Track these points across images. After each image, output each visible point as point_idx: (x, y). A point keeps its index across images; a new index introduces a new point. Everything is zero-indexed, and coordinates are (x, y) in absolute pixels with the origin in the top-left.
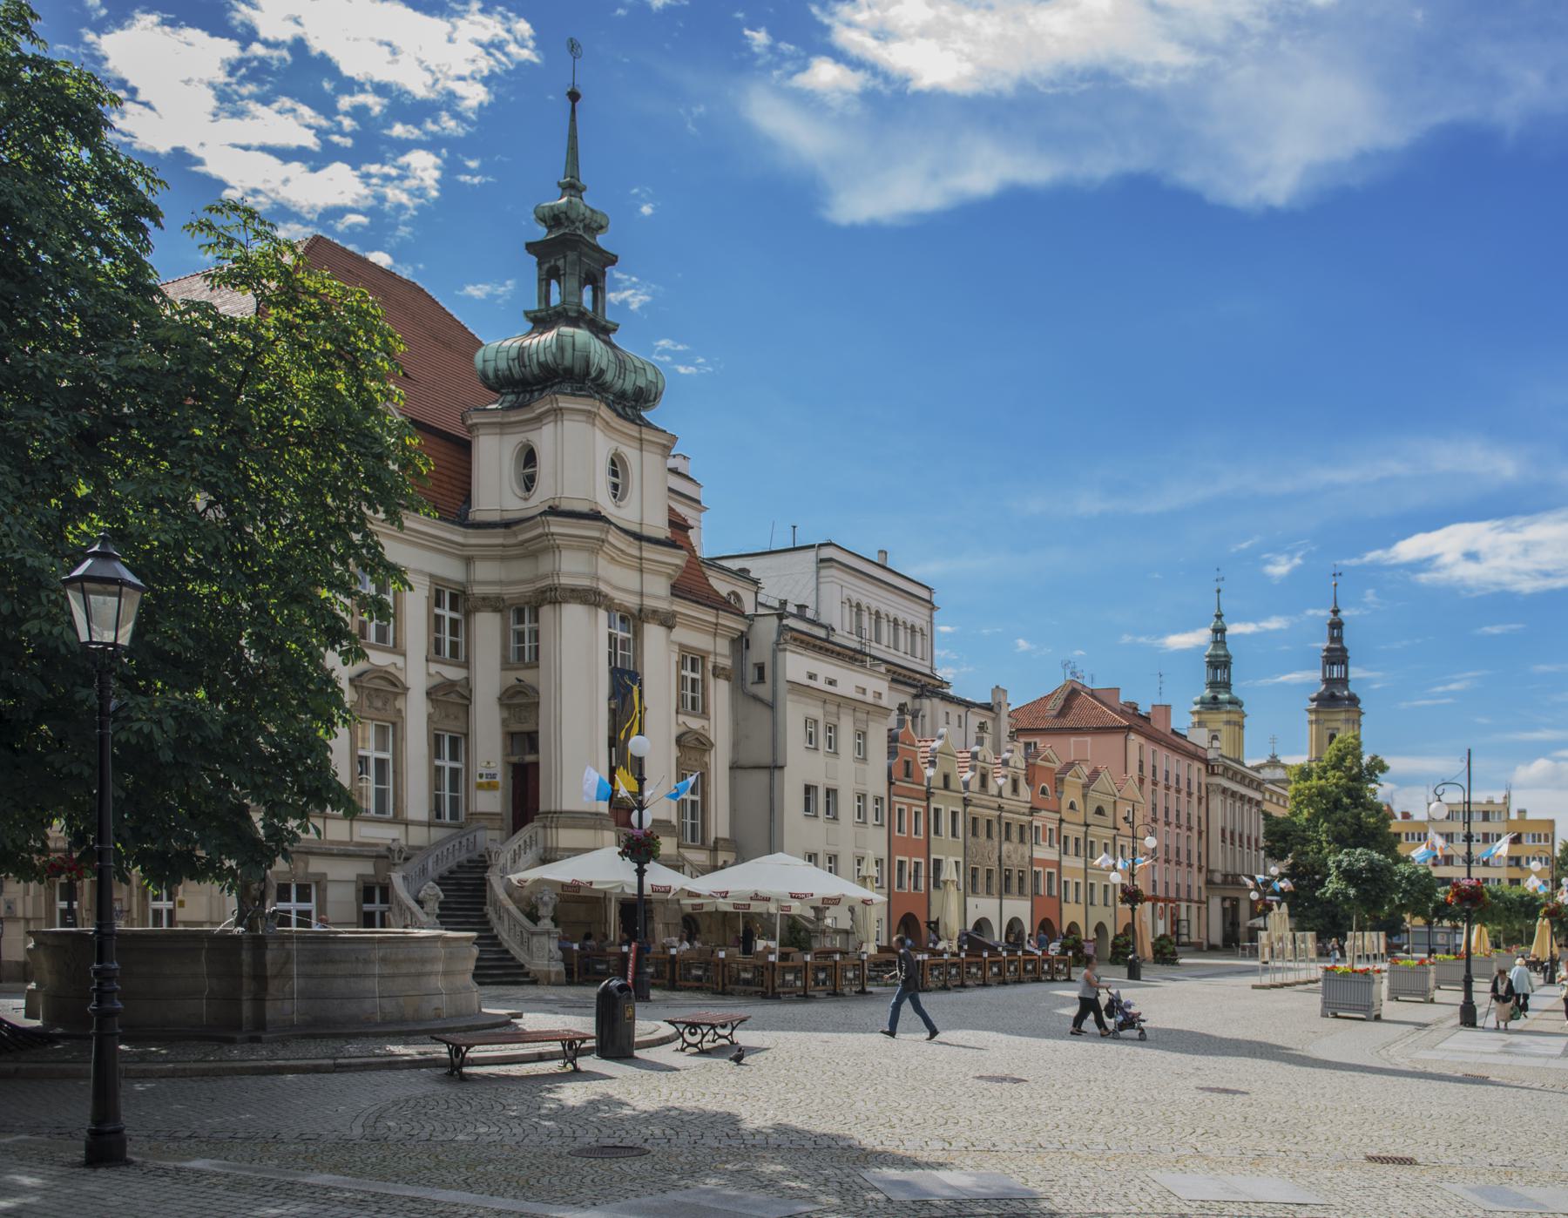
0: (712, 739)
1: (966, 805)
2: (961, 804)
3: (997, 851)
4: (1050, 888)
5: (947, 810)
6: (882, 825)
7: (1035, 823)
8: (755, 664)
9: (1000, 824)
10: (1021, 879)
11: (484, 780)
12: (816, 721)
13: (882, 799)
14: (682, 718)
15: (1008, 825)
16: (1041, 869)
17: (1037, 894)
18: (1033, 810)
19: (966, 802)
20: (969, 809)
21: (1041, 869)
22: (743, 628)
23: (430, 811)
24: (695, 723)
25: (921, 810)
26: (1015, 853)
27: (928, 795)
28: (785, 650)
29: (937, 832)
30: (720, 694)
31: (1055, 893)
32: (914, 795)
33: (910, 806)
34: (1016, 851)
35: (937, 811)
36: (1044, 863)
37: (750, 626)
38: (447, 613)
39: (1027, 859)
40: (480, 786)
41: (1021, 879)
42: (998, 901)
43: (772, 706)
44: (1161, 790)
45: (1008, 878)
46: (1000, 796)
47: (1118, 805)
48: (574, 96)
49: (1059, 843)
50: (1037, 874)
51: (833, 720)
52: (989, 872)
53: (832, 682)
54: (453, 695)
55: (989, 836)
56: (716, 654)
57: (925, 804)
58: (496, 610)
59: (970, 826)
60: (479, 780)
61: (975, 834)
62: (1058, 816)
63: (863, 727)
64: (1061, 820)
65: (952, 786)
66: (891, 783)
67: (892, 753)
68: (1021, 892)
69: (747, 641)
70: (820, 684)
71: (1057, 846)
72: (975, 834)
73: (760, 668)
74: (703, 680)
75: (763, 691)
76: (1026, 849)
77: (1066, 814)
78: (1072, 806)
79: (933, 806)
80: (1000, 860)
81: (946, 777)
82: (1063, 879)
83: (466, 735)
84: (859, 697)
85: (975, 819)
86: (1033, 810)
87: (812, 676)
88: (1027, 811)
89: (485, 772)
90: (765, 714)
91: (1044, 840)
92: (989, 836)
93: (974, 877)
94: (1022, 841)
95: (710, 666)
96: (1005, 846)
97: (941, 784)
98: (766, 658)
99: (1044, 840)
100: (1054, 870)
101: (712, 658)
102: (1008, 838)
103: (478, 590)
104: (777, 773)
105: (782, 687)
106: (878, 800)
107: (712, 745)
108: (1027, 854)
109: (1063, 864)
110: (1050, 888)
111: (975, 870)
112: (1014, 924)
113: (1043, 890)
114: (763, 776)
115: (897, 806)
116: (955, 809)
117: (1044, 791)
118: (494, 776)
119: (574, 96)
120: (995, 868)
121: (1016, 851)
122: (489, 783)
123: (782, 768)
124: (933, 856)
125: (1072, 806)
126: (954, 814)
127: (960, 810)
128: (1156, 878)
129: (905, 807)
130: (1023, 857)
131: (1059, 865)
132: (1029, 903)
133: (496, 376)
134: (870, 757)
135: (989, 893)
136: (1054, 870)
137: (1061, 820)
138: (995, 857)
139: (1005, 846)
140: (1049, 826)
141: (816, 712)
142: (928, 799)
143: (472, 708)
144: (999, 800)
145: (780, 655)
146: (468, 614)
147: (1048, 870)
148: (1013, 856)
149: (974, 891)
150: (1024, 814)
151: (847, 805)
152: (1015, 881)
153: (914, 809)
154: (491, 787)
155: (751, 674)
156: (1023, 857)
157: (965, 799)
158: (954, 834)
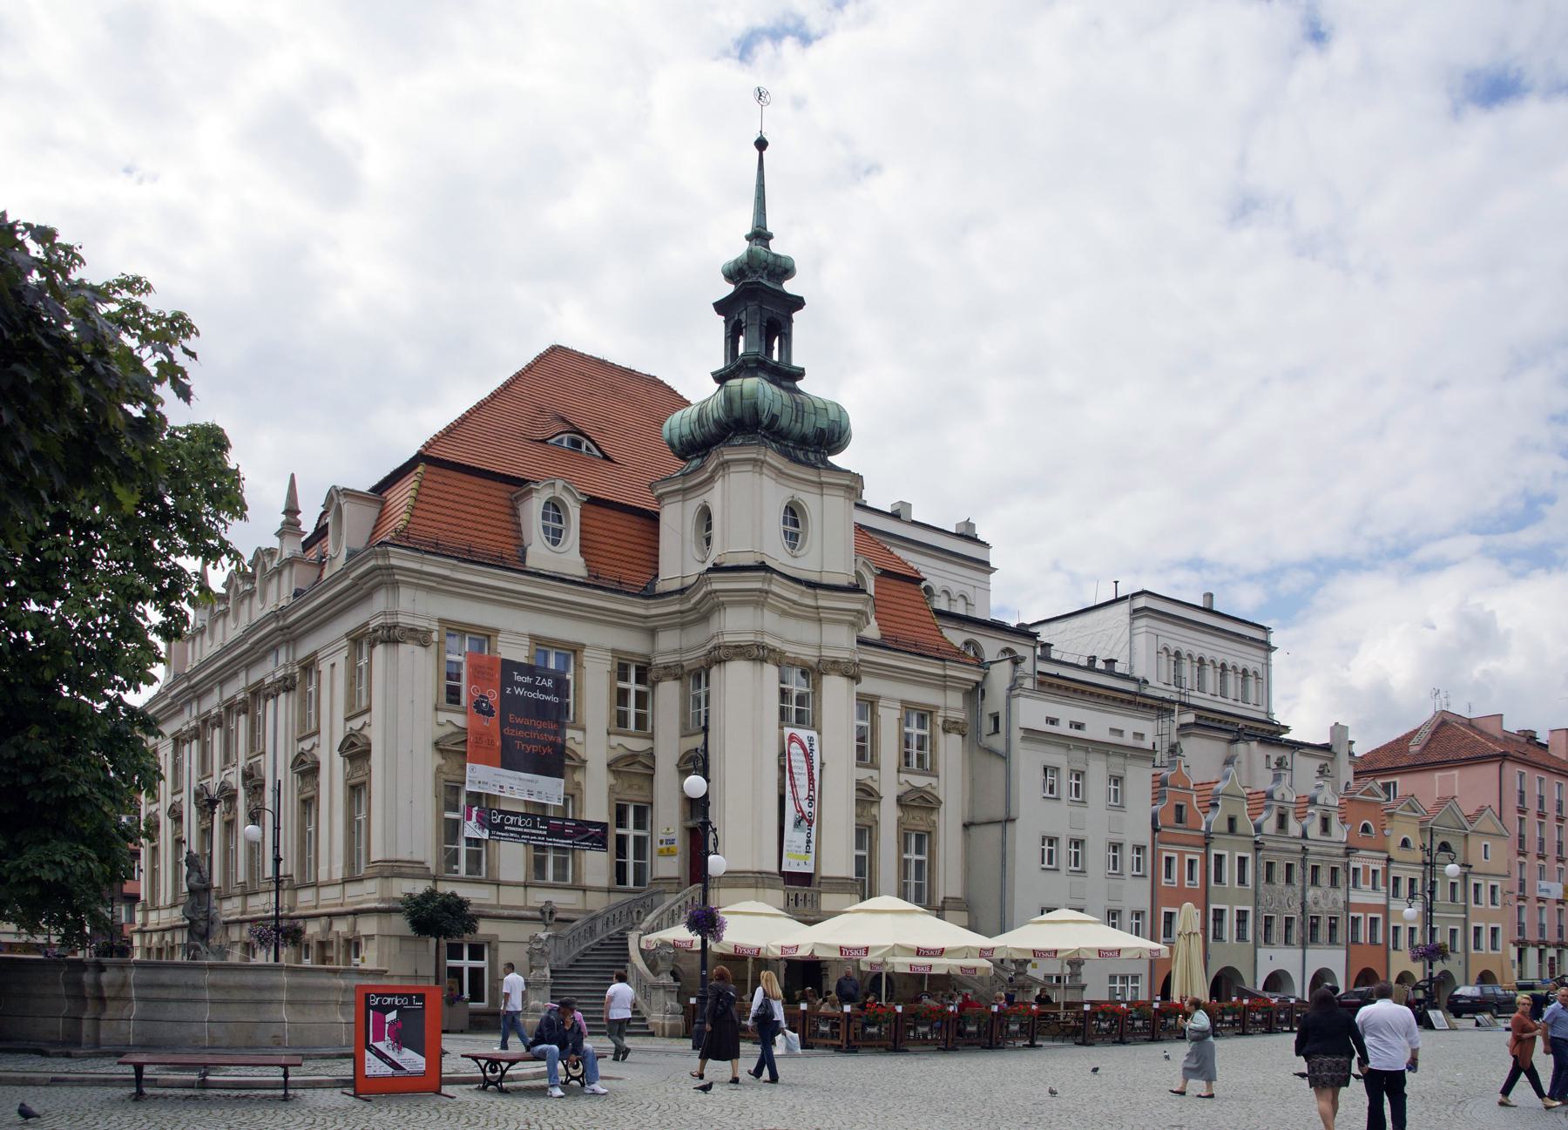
0: (941, 798)
1: (1257, 850)
2: (1251, 846)
3: (1300, 896)
4: (1373, 934)
5: (1232, 855)
6: (1144, 876)
7: (1353, 865)
8: (990, 715)
9: (1304, 868)
10: (1333, 927)
11: (664, 846)
12: (1058, 769)
13: (1144, 847)
14: (903, 777)
15: (1315, 868)
16: (1361, 915)
17: (1355, 941)
18: (1349, 851)
19: (1258, 847)
20: (1261, 854)
22: (978, 678)
23: (611, 877)
24: (920, 781)
25: (1197, 857)
26: (1323, 899)
27: (1207, 840)
28: (1018, 695)
29: (1218, 879)
30: (950, 749)
31: (1380, 939)
32: (1186, 842)
34: (1325, 896)
35: (1219, 858)
36: (1366, 908)
37: (985, 676)
38: (632, 686)
39: (1341, 905)
40: (661, 853)
41: (1333, 927)
42: (1301, 951)
43: (1005, 757)
44: (1531, 818)
45: (1314, 927)
46: (1304, 836)
47: (1470, 838)
48: (761, 144)
49: (1386, 884)
50: (1355, 921)
51: (1079, 767)
52: (1289, 921)
53: (1079, 726)
54: (636, 766)
55: (1289, 880)
56: (946, 709)
57: (1202, 851)
58: (678, 678)
59: (1263, 871)
60: (660, 846)
61: (1269, 879)
62: (1385, 855)
63: (1118, 772)
64: (1389, 860)
65: (1240, 828)
66: (1155, 830)
67: (1158, 797)
68: (1332, 940)
69: (983, 691)
70: (1063, 729)
71: (1383, 889)
72: (1269, 879)
73: (996, 718)
74: (931, 737)
75: (998, 743)
76: (1340, 895)
77: (1395, 852)
78: (1405, 843)
79: (1213, 852)
80: (1303, 905)
81: (1232, 821)
83: (652, 804)
84: (1115, 739)
85: (1270, 865)
86: (1349, 851)
87: (1053, 721)
88: (1341, 851)
89: (664, 837)
90: (998, 767)
91: (1366, 882)
92: (1289, 880)
93: (1268, 926)
94: (1334, 883)
95: (940, 721)
96: (1311, 893)
97: (1225, 828)
98: (1000, 707)
99: (1366, 882)
100: (1379, 915)
101: (941, 713)
102: (1315, 882)
103: (659, 660)
104: (1009, 826)
105: (1017, 735)
106: (1139, 849)
107: (940, 802)
109: (1391, 907)
110: (1373, 934)
111: (1268, 920)
113: (1364, 935)
114: (995, 831)
115: (1165, 854)
116: (1243, 854)
117: (1366, 828)
118: (672, 842)
119: (761, 144)
120: (1297, 916)
121: (1325, 896)
122: (668, 849)
123: (1013, 820)
125: (1405, 843)
126: (1242, 860)
127: (1249, 855)
128: (1545, 921)
129: (1175, 855)
130: (1335, 902)
131: (1385, 909)
132: (1343, 953)
133: (681, 443)
134: (1129, 804)
135: (1287, 941)
137: (1389, 860)
138: (1297, 906)
139: (1311, 893)
140: (1373, 867)
141: (1057, 757)
142: (1207, 845)
143: (655, 777)
144: (1302, 841)
145: (1014, 701)
146: (654, 685)
147: (1370, 915)
148: (1322, 902)
149: (1267, 940)
150: (1337, 856)
151: (1097, 855)
152: (1323, 931)
153: (1188, 857)
154: (669, 853)
155: (988, 725)
157: (1256, 842)
158: (1242, 881)
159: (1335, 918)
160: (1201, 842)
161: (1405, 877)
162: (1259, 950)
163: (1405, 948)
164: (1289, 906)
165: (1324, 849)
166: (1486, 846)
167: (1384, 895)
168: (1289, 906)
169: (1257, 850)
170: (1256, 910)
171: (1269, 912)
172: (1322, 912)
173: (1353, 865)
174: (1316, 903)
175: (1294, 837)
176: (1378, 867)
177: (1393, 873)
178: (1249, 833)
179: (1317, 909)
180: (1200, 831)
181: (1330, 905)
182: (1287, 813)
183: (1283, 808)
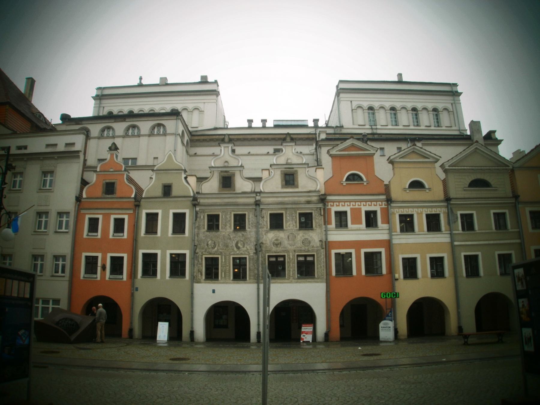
1: (195, 205)
3: (253, 239)
25: (126, 217)
36: (358, 245)
42: (255, 285)
88: (315, 199)
109: (395, 241)
130: (306, 242)
131: (388, 244)
136: (383, 250)
160: (132, 206)
162: (196, 285)
163: (424, 276)
164: (238, 248)
165: (286, 199)
167: (387, 231)
168: (238, 248)
169: (195, 205)
170: (194, 253)
171: (210, 254)
172: (288, 251)
173: (334, 209)
178: (189, 195)
179: (280, 249)
180: (130, 198)
182: (234, 175)
183: (226, 172)
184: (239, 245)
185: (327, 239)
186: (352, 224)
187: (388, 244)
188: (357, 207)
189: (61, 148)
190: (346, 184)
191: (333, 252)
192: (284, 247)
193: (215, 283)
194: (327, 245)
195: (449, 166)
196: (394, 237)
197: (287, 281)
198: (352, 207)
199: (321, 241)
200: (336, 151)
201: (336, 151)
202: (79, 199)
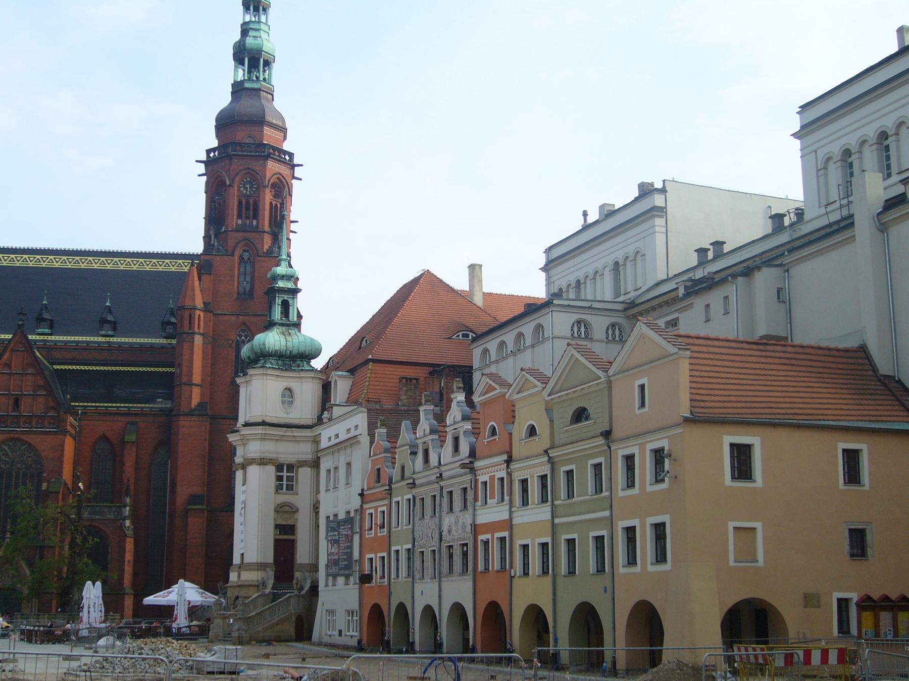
16: (489, 536)
21: (489, 536)
33: (376, 508)
39: (469, 528)
76: (467, 518)
79: (394, 500)
82: (519, 542)
108: (469, 521)
112: (458, 610)
115: (368, 511)
124: (394, 548)
129: (372, 511)
131: (509, 524)
132: (471, 583)
153: (380, 509)
156: (464, 527)
159: (466, 545)
161: (532, 477)
166: (642, 387)
173: (482, 478)
174: (450, 532)
175: (435, 467)
176: (503, 474)
177: (517, 476)
181: (460, 531)
184: (433, 536)
185: (474, 523)
186: (490, 499)
187: (509, 524)
188: (493, 474)
189: (343, 436)
190: (488, 442)
191: (481, 537)
192: (453, 535)
193: (422, 582)
194: (476, 529)
195: (548, 396)
196: (515, 515)
197: (454, 578)
198: (490, 474)
199: (471, 524)
200: (479, 396)
201: (479, 396)
202: (361, 495)
